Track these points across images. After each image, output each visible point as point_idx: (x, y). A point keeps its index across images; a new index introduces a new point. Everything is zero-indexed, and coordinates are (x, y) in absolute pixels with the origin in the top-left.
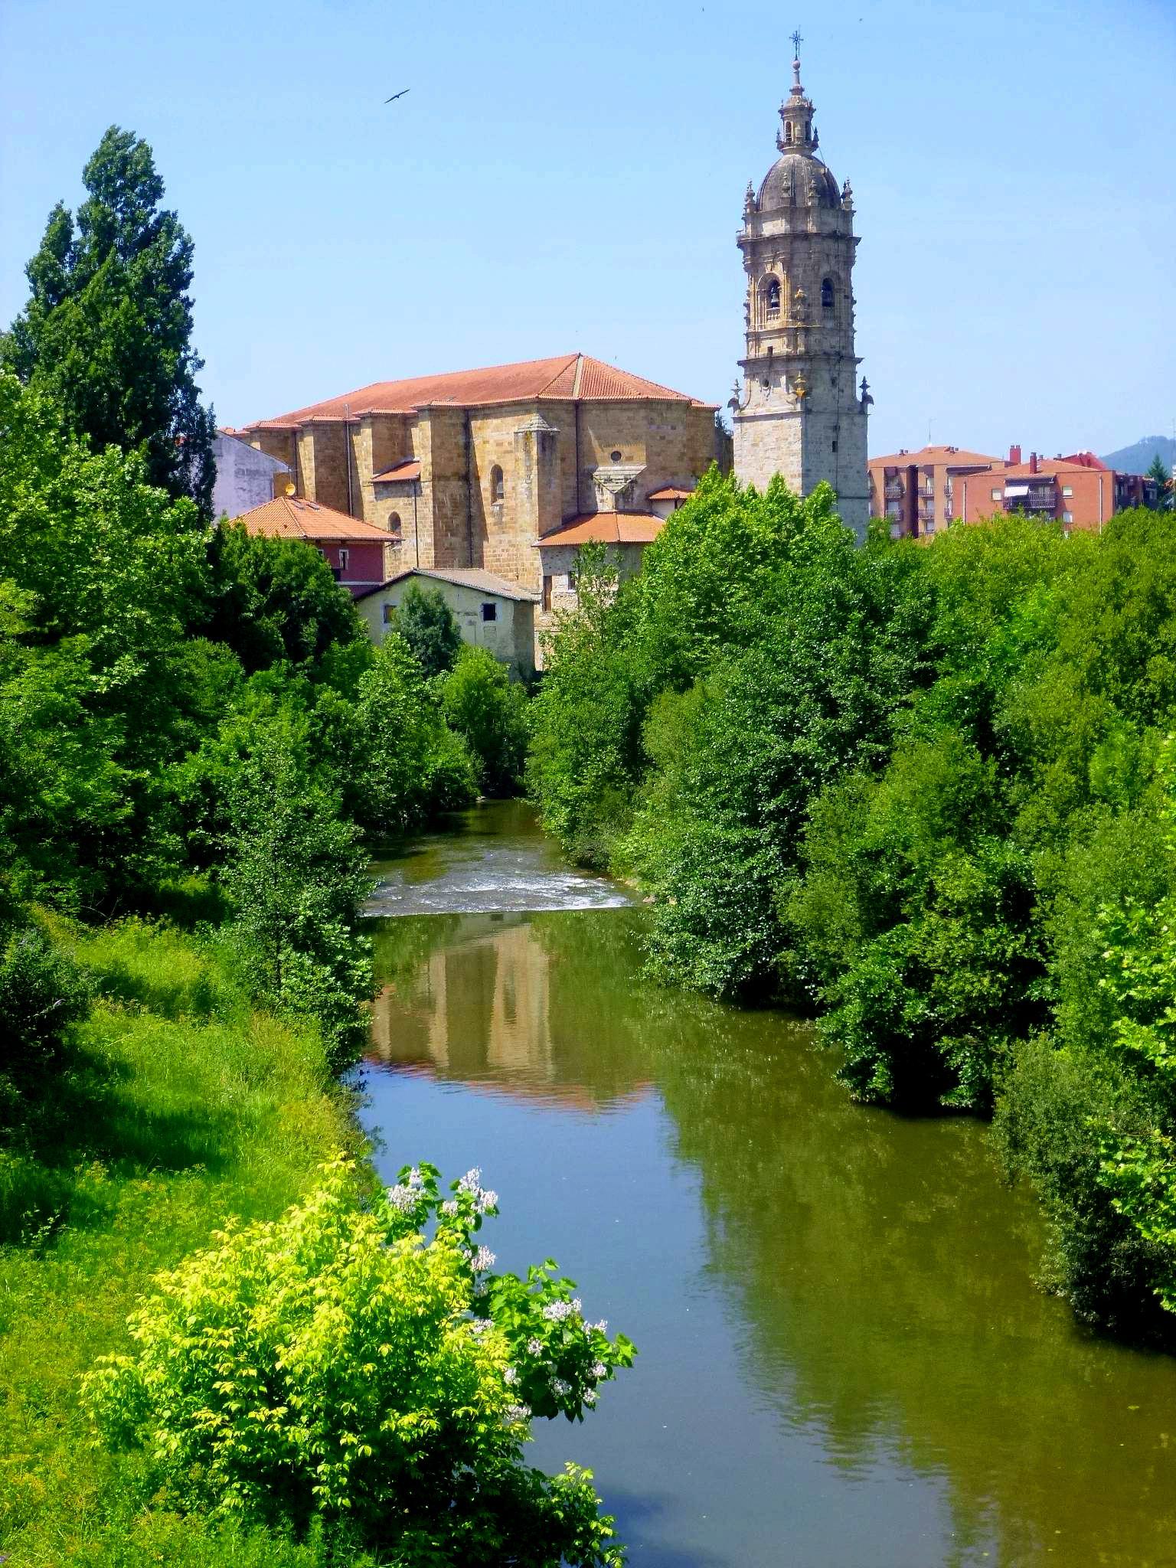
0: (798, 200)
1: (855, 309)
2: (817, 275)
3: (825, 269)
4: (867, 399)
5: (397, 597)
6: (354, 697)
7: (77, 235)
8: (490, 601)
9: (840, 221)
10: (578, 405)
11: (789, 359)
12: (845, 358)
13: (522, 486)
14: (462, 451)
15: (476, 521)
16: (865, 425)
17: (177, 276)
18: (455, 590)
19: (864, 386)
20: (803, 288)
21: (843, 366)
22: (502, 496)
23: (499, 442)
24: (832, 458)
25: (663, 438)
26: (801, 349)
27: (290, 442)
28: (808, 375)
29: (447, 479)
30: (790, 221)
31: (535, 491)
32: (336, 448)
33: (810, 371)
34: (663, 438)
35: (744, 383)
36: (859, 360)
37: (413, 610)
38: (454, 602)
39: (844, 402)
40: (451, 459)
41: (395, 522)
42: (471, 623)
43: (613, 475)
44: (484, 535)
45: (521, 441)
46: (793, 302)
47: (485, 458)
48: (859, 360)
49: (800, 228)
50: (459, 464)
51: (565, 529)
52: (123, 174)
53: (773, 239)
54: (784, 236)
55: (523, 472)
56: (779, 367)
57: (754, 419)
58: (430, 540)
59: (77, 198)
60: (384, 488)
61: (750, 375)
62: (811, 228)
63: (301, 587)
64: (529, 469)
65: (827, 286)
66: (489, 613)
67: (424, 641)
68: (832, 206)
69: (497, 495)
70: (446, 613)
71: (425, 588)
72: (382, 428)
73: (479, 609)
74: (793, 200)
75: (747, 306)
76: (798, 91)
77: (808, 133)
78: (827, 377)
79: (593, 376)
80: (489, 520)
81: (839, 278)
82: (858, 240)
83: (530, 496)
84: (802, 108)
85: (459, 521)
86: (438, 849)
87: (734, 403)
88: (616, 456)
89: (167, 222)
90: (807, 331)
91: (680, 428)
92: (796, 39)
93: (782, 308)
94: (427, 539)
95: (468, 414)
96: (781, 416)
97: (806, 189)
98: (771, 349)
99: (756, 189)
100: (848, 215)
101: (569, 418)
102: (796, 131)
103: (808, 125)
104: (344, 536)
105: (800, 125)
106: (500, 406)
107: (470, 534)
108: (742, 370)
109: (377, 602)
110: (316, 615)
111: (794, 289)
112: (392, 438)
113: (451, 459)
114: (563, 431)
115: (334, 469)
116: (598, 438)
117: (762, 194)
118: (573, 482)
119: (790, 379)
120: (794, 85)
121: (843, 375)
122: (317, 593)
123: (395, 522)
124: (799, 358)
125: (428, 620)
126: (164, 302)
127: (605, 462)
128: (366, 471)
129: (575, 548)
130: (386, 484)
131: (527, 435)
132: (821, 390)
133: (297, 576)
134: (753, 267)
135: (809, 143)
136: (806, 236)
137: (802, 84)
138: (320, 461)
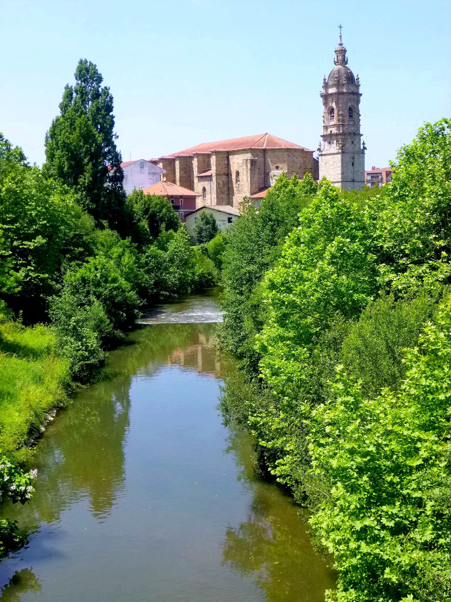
0: (341, 81)
1: (360, 118)
2: (347, 107)
3: (350, 104)
4: (365, 148)
5: (198, 215)
6: (165, 250)
7: (74, 95)
8: (230, 216)
9: (355, 88)
10: (265, 150)
11: (337, 135)
12: (357, 134)
13: (245, 178)
14: (226, 166)
15: (231, 189)
16: (364, 157)
17: (109, 108)
18: (218, 213)
19: (364, 144)
20: (342, 110)
21: (356, 137)
22: (239, 181)
23: (238, 163)
25: (293, 161)
26: (341, 131)
27: (173, 163)
28: (343, 140)
29: (221, 175)
30: (338, 88)
31: (249, 179)
32: (186, 165)
33: (344, 139)
34: (293, 161)
35: (323, 143)
36: (362, 135)
37: (202, 219)
38: (217, 216)
39: (356, 149)
40: (222, 169)
41: (204, 189)
42: (224, 224)
43: (276, 175)
44: (233, 195)
45: (245, 163)
46: (339, 115)
47: (234, 168)
48: (362, 135)
49: (341, 90)
50: (225, 171)
51: (259, 192)
52: (87, 73)
53: (332, 94)
54: (335, 93)
55: (245, 173)
56: (334, 138)
57: (325, 155)
58: (215, 196)
59: (73, 83)
60: (201, 178)
61: (324, 140)
62: (345, 91)
63: (160, 212)
64: (247, 172)
65: (350, 109)
66: (230, 220)
67: (206, 230)
68: (352, 83)
69: (237, 181)
70: (214, 221)
71: (207, 212)
72: (201, 158)
73: (227, 219)
74: (338, 81)
75: (324, 117)
76: (341, 44)
78: (350, 141)
79: (271, 141)
80: (235, 189)
82: (361, 95)
83: (247, 181)
84: (342, 50)
85: (225, 189)
86: (195, 301)
87: (319, 150)
88: (277, 168)
89: (106, 90)
90: (343, 125)
91: (299, 158)
92: (340, 27)
93: (335, 117)
94: (214, 195)
95: (228, 154)
96: (334, 154)
97: (343, 77)
98: (331, 131)
99: (327, 78)
100: (358, 86)
101: (261, 155)
102: (340, 58)
103: (344, 56)
104: (181, 194)
105: (342, 56)
106: (238, 151)
107: (229, 194)
108: (322, 138)
109: (193, 216)
110: (165, 221)
111: (339, 111)
112: (204, 161)
113: (222, 169)
114: (259, 159)
115: (186, 172)
116: (271, 162)
117: (328, 79)
118: (263, 176)
119: (337, 141)
120: (340, 42)
121: (356, 140)
122: (166, 214)
123: (204, 189)
124: (340, 134)
125: (207, 223)
126: (104, 117)
127: (274, 170)
128: (196, 173)
129: (262, 198)
130: (201, 177)
131: (247, 160)
132: (348, 145)
133: (159, 208)
134: (326, 104)
135: (344, 62)
136: (343, 93)
137: (343, 42)
138: (181, 170)
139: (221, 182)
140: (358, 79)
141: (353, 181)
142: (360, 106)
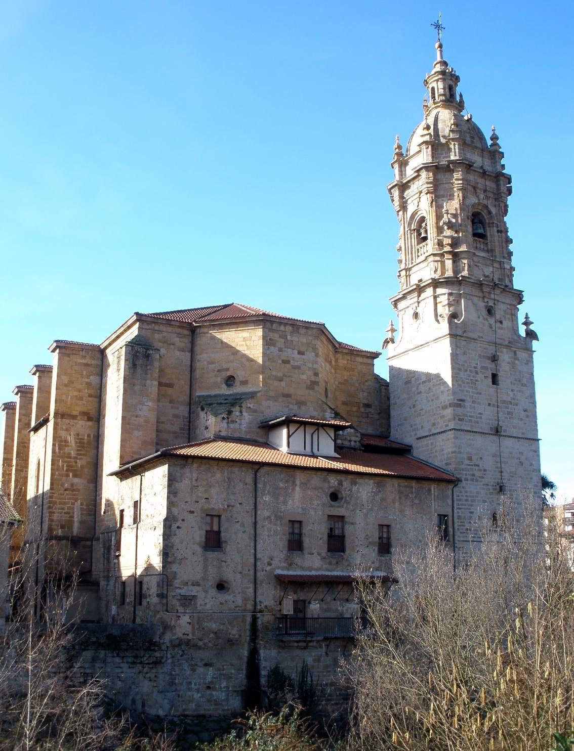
4: (531, 335)
16: (530, 362)
19: (527, 323)
21: (497, 295)
24: (492, 390)
25: (288, 362)
29: (74, 417)
39: (504, 334)
40: (81, 399)
46: (440, 230)
50: (88, 405)
81: (490, 212)
92: (438, 26)
93: (428, 241)
113: (81, 399)
135: (452, 100)
139: (71, 439)
140: (494, 138)
141: (497, 431)
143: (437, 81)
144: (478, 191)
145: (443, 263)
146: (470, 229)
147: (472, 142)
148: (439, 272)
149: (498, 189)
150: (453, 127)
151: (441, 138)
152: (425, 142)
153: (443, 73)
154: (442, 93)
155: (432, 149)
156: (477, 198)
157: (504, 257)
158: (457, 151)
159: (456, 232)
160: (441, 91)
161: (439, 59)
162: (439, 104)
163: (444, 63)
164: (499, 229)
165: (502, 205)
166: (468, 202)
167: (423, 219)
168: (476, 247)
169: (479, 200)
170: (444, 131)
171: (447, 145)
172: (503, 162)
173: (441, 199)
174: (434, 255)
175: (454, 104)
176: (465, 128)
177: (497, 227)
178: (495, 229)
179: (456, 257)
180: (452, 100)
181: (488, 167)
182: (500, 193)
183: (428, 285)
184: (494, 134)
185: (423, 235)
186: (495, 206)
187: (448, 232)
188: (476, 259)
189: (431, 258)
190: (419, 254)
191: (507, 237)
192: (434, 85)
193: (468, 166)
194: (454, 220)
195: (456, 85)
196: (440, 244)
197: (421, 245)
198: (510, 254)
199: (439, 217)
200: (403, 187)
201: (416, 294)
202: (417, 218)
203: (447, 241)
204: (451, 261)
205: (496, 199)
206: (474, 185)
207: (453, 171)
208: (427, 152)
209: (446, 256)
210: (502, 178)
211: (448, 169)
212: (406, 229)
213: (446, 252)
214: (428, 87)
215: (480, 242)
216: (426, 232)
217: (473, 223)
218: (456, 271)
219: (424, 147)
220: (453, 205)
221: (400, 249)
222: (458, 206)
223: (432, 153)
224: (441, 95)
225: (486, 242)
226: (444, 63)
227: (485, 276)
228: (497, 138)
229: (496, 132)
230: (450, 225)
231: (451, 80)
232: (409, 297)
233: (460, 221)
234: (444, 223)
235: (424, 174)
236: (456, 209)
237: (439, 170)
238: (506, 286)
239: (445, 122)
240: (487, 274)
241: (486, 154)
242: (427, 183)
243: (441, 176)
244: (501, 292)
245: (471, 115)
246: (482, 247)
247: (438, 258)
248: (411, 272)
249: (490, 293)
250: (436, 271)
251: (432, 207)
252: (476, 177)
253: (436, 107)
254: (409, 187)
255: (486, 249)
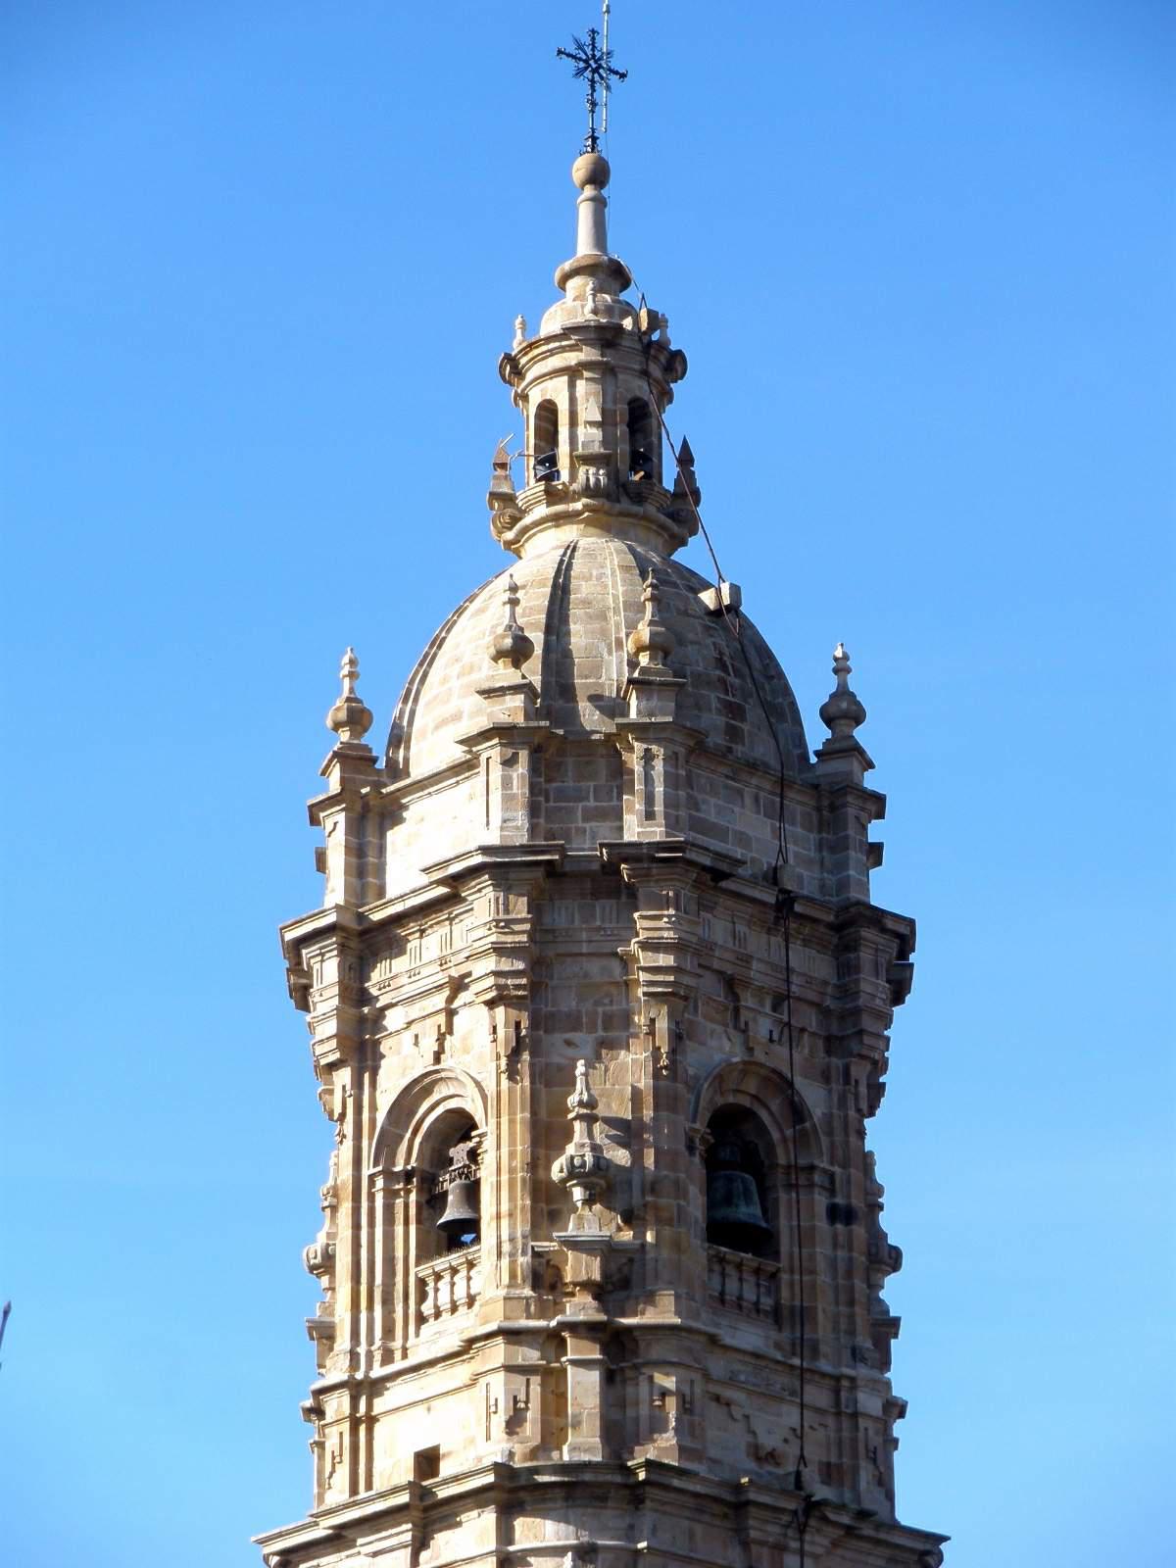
1: (894, 1292)
46: (546, 1204)
77: (644, 458)
81: (797, 1112)
92: (592, 64)
98: (428, 1461)
135: (642, 492)
140: (843, 712)
142: (879, 1134)
143: (573, 373)
144: (748, 1000)
145: (553, 1380)
146: (696, 1204)
147: (733, 733)
148: (531, 1429)
149: (847, 991)
150: (644, 659)
151: (584, 707)
152: (501, 732)
153: (606, 336)
154: (597, 449)
155: (534, 770)
156: (737, 1038)
157: (856, 1355)
158: (659, 790)
159: (629, 1218)
160: (590, 437)
161: (584, 247)
162: (578, 506)
163: (611, 275)
164: (839, 1200)
165: (860, 1071)
166: (695, 1059)
167: (460, 1126)
168: (722, 1299)
169: (750, 1050)
170: (596, 669)
171: (610, 750)
172: (875, 831)
173: (558, 1038)
174: (512, 1335)
175: (651, 509)
176: (700, 656)
177: (832, 1191)
178: (821, 1201)
179: (621, 1353)
180: (642, 492)
181: (804, 878)
182: (857, 1012)
183: (476, 1498)
184: (843, 693)
185: (450, 1214)
186: (826, 1077)
187: (590, 1222)
188: (718, 1365)
189: (497, 1353)
190: (427, 1308)
191: (877, 1236)
192: (557, 390)
193: (697, 873)
194: (621, 1156)
195: (666, 396)
196: (545, 1278)
197: (441, 1263)
198: (889, 1326)
199: (547, 1133)
200: (367, 941)
201: (404, 1533)
202: (429, 1114)
203: (579, 1268)
204: (594, 1377)
205: (832, 1043)
206: (729, 970)
207: (630, 897)
208: (506, 783)
209: (577, 1349)
210: (868, 934)
211: (616, 880)
212: (367, 1170)
213: (573, 1327)
214: (525, 397)
215: (739, 1266)
216: (472, 1193)
217: (712, 1163)
218: (619, 1433)
219: (492, 752)
220: (626, 1075)
221: (326, 1264)
222: (645, 1083)
223: (534, 789)
224: (588, 460)
225: (770, 1266)
226: (611, 275)
227: (764, 1457)
228: (857, 716)
229: (854, 684)
230: (602, 1183)
231: (645, 374)
232: (367, 1543)
233: (649, 1160)
234: (573, 1172)
235: (483, 901)
236: (636, 1096)
237: (555, 884)
238: (863, 1515)
239: (602, 616)
240: (769, 1441)
241: (799, 803)
242: (499, 950)
243: (565, 915)
244: (835, 1544)
245: (735, 591)
246: (750, 1294)
247: (530, 1355)
248: (380, 1405)
249: (780, 1548)
250: (513, 1424)
251: (512, 1073)
252: (741, 928)
253: (558, 520)
254: (397, 948)
255: (767, 1302)
